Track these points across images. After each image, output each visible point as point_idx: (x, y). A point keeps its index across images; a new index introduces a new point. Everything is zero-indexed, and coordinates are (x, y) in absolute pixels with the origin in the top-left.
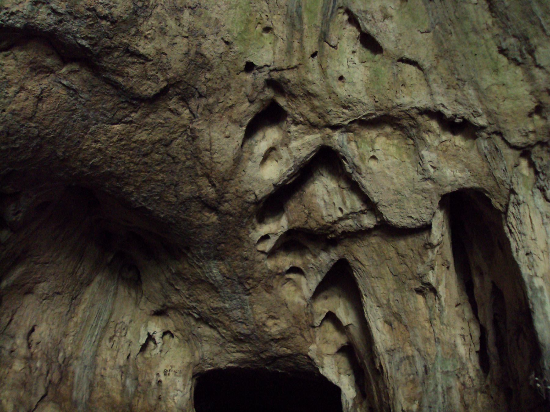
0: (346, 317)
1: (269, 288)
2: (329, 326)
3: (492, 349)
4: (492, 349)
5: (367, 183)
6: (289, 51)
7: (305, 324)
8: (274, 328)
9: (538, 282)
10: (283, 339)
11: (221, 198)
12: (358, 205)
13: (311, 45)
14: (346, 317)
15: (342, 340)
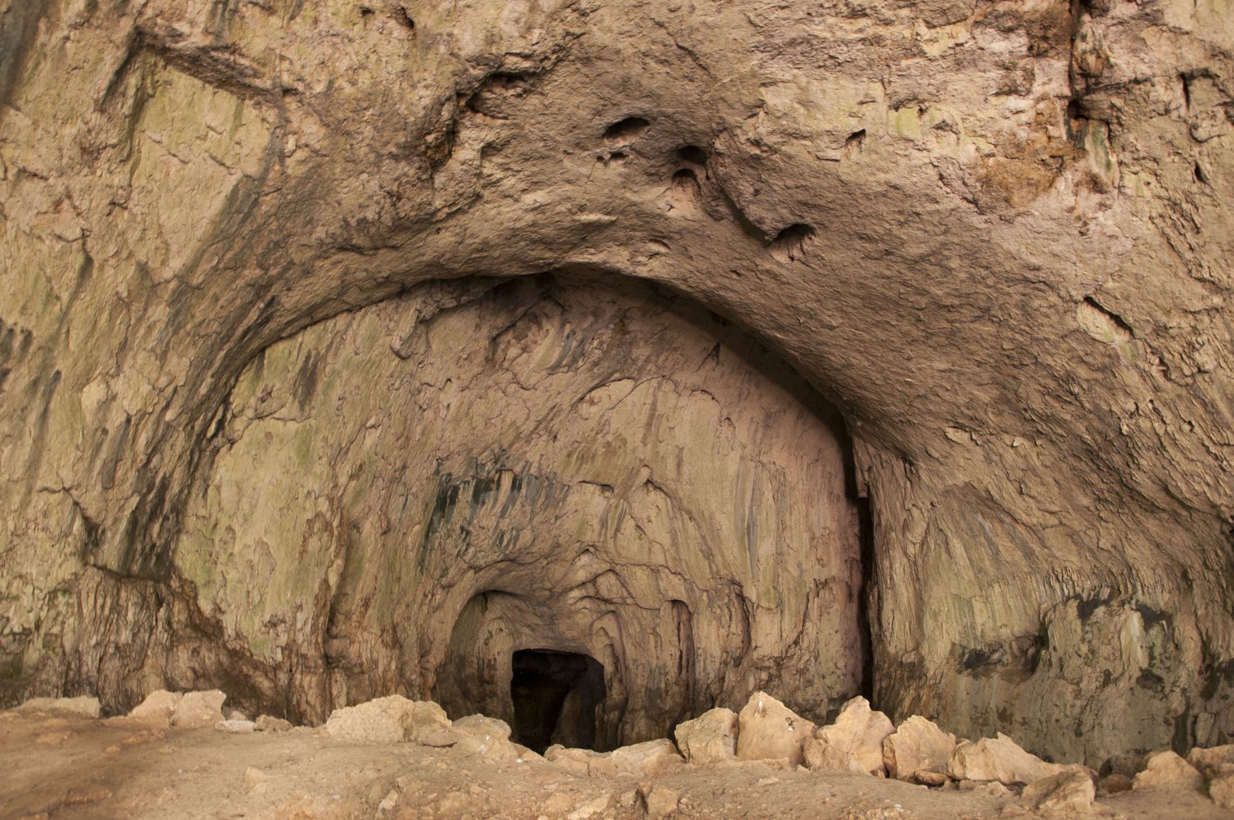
0: (613, 632)
1: (569, 617)
2: (601, 632)
3: (684, 663)
4: (684, 663)
5: (631, 590)
6: (600, 535)
7: (589, 632)
8: (569, 634)
9: (700, 651)
10: (574, 639)
11: (554, 587)
12: (625, 594)
13: (610, 533)
14: (613, 632)
15: (608, 642)
